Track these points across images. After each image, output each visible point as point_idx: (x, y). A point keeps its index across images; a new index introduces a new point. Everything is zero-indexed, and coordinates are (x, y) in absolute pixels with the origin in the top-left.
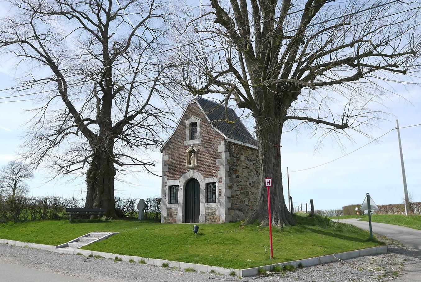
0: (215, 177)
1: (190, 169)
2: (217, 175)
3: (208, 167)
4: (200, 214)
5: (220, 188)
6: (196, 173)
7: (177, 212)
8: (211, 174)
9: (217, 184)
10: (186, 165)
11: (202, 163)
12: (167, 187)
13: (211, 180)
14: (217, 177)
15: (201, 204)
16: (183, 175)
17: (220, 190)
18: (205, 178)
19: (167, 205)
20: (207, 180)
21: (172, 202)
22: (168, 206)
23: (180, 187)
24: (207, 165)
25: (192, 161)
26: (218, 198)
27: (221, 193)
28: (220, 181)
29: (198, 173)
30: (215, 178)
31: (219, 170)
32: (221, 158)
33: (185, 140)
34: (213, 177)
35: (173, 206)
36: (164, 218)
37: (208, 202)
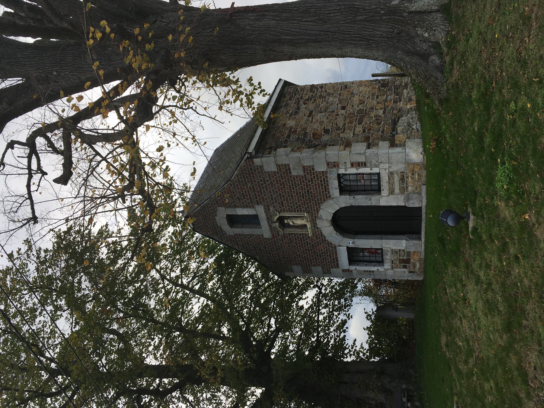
0: (327, 177)
1: (314, 226)
2: (323, 172)
3: (308, 191)
4: (403, 204)
5: (349, 165)
6: (321, 215)
8: (322, 185)
9: (342, 171)
10: (308, 234)
11: (302, 204)
12: (353, 268)
13: (334, 184)
14: (326, 172)
16: (327, 239)
17: (352, 165)
18: (330, 196)
19: (387, 269)
20: (335, 191)
21: (380, 259)
22: (387, 266)
23: (351, 245)
24: (305, 192)
25: (299, 222)
27: (359, 163)
28: (335, 166)
29: (321, 211)
30: (328, 175)
31: (313, 169)
32: (289, 165)
33: (262, 235)
34: (327, 181)
35: (388, 257)
36: (411, 274)
37: (378, 190)
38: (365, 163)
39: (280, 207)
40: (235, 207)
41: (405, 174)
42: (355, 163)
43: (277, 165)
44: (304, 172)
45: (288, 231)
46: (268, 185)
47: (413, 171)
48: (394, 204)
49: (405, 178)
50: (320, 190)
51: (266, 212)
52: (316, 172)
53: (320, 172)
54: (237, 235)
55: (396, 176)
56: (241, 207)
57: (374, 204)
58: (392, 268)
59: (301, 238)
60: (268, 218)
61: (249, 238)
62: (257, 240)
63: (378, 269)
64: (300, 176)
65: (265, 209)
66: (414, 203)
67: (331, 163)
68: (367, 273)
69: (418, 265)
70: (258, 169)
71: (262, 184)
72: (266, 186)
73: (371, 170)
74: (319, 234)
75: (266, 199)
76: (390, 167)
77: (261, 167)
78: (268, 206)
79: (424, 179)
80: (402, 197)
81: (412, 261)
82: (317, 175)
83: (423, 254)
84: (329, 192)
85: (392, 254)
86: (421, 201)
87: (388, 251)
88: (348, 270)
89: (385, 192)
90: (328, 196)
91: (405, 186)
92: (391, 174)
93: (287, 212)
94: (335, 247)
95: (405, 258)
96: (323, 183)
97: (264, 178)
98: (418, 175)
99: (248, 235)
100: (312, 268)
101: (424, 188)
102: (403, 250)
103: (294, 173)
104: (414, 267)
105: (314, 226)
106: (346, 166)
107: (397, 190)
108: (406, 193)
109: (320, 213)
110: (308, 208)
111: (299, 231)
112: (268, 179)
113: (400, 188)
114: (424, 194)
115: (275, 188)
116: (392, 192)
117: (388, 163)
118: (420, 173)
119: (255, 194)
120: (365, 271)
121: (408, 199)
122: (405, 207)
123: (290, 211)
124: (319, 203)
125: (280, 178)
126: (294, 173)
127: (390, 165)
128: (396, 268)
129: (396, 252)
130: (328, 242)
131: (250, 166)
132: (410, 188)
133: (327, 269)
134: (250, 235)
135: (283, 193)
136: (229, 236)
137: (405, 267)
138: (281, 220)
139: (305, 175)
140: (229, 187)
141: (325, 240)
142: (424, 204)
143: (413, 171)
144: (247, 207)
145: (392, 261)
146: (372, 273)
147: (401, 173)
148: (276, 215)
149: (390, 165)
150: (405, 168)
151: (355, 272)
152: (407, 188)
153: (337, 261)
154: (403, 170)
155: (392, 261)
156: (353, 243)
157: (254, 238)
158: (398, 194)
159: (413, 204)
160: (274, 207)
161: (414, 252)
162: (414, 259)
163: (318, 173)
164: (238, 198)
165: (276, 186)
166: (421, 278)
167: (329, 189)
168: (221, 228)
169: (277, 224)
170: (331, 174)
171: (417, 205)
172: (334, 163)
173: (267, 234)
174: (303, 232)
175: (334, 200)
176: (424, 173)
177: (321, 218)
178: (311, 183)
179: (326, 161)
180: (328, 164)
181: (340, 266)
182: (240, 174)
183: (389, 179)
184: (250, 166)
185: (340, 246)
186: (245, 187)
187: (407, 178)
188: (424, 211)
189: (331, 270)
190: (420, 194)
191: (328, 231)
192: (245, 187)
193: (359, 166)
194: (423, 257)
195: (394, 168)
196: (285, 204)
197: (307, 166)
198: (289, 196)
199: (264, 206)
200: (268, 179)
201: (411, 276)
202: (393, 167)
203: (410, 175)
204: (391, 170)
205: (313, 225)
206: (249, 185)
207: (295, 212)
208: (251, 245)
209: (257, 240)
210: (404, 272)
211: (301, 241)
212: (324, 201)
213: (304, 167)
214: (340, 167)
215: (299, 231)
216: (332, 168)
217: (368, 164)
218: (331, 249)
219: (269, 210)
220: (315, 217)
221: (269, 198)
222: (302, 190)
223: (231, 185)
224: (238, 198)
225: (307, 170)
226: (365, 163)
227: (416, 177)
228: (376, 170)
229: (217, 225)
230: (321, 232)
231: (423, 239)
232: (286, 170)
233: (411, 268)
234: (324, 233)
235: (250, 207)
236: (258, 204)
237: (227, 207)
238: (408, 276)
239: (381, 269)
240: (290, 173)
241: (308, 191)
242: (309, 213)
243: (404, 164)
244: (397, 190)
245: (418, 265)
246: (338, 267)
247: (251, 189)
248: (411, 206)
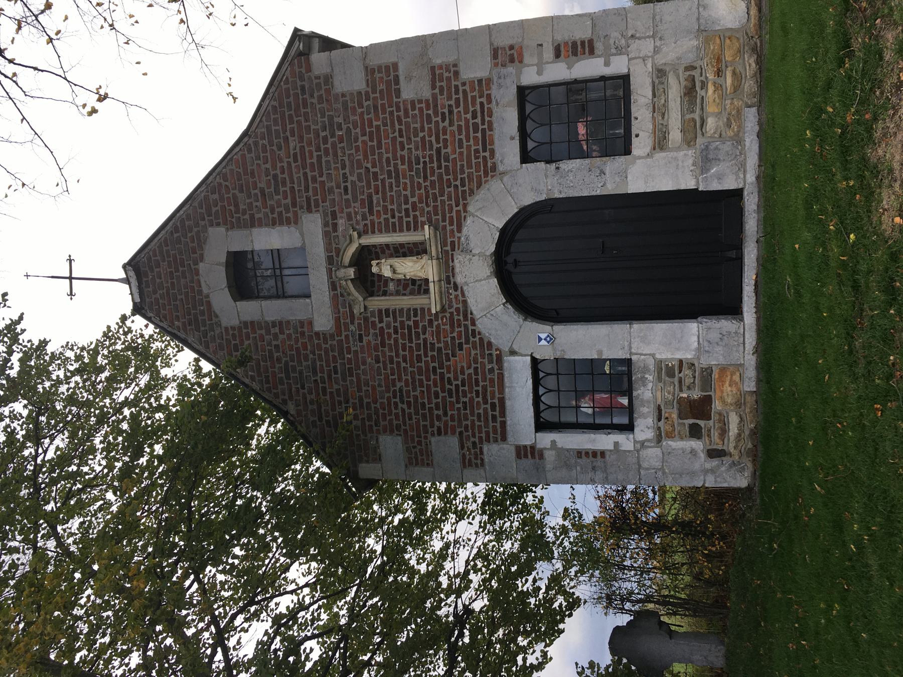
0: (489, 97)
2: (480, 81)
3: (438, 151)
5: (549, 54)
7: (681, 361)
8: (475, 126)
9: (530, 77)
10: (429, 309)
11: (421, 202)
12: (545, 439)
13: (507, 120)
14: (489, 81)
15: (637, 184)
17: (558, 55)
18: (494, 168)
19: (642, 443)
20: (508, 151)
21: (625, 421)
22: (644, 429)
23: (544, 352)
24: (431, 156)
25: (409, 267)
26: (601, 61)
27: (574, 44)
28: (512, 60)
29: (469, 220)
30: (495, 92)
31: (456, 74)
32: (395, 66)
33: (310, 323)
35: (647, 392)
36: (715, 462)
37: (622, 146)
38: (591, 42)
39: (364, 218)
40: (253, 223)
41: (696, 73)
42: (566, 44)
44: (433, 87)
45: (378, 303)
47: (719, 60)
48: (666, 184)
49: (698, 85)
50: (469, 147)
51: (326, 234)
52: (464, 84)
53: (472, 82)
54: (245, 323)
55: (672, 80)
56: (267, 225)
57: (611, 188)
58: (659, 439)
59: (409, 328)
60: (330, 260)
61: (276, 336)
62: (297, 341)
63: (616, 444)
64: (420, 102)
65: (326, 224)
66: (721, 179)
67: (504, 49)
68: (584, 461)
72: (334, 146)
73: (607, 64)
75: (331, 191)
76: (657, 50)
77: (328, 79)
78: (334, 216)
79: (749, 85)
80: (688, 157)
81: (717, 406)
82: (465, 91)
83: (751, 372)
84: (492, 152)
85: (660, 379)
86: (743, 166)
87: (646, 369)
88: (533, 447)
89: (641, 145)
90: (490, 170)
91: (696, 116)
92: (660, 73)
93: (380, 231)
95: (696, 394)
96: (478, 120)
97: (331, 118)
99: (274, 324)
100: (433, 440)
101: (751, 118)
102: (692, 365)
103: (408, 92)
104: (724, 432)
106: (540, 55)
107: (675, 135)
108: (700, 140)
109: (465, 230)
110: (436, 214)
112: (341, 120)
113: (683, 122)
114: (751, 144)
116: (660, 143)
117: (653, 36)
118: (739, 69)
119: (305, 174)
120: (579, 453)
121: (705, 161)
123: (387, 231)
124: (464, 192)
125: (372, 115)
126: (408, 92)
127: (658, 43)
128: (670, 436)
129: (670, 373)
130: (481, 339)
131: (302, 78)
132: (711, 122)
133: (474, 443)
134: (281, 323)
135: (374, 166)
136: (226, 329)
137: (695, 432)
138: (364, 258)
139: (434, 97)
140: (243, 156)
141: (473, 331)
142: (751, 177)
143: (719, 60)
144: (281, 224)
146: (599, 462)
149: (658, 43)
151: (550, 456)
153: (503, 413)
154: (690, 58)
157: (289, 337)
158: (678, 149)
159: (720, 177)
160: (349, 217)
161: (723, 369)
162: (724, 396)
163: (467, 88)
164: (262, 191)
165: (359, 143)
166: (741, 481)
167: (492, 143)
168: (209, 304)
169: (351, 272)
170: (500, 86)
171: (730, 184)
172: (511, 47)
173: (323, 322)
174: (417, 301)
175: (505, 179)
176: (750, 64)
179: (491, 44)
180: (495, 53)
181: (510, 438)
182: (274, 107)
183: (654, 95)
184: (302, 78)
185: (513, 353)
186: (282, 153)
187: (704, 85)
188: (751, 203)
190: (738, 140)
192: (282, 153)
193: (575, 54)
194: (750, 385)
196: (378, 203)
197: (440, 67)
198: (390, 177)
199: (325, 215)
200: (341, 120)
201: (712, 471)
202: (665, 49)
203: (711, 76)
204: (660, 60)
205: (444, 277)
206: (292, 145)
207: (401, 230)
208: (279, 360)
209: (297, 341)
210: (693, 452)
211: (411, 341)
213: (433, 69)
214: (527, 59)
216: (504, 65)
217: (599, 46)
219: (335, 226)
220: (453, 243)
221: (338, 187)
222: (424, 149)
223: (250, 151)
224: (262, 191)
225: (441, 75)
226: (591, 42)
228: (618, 66)
229: (200, 292)
230: (465, 302)
232: (388, 83)
233: (715, 435)
234: (471, 302)
235: (288, 222)
236: (309, 210)
237: (232, 227)
238: (706, 472)
239: (625, 441)
240: (398, 92)
241: (438, 151)
242: (436, 229)
243: (697, 37)
244: (675, 135)
246: (504, 438)
247: (296, 161)
248: (715, 186)
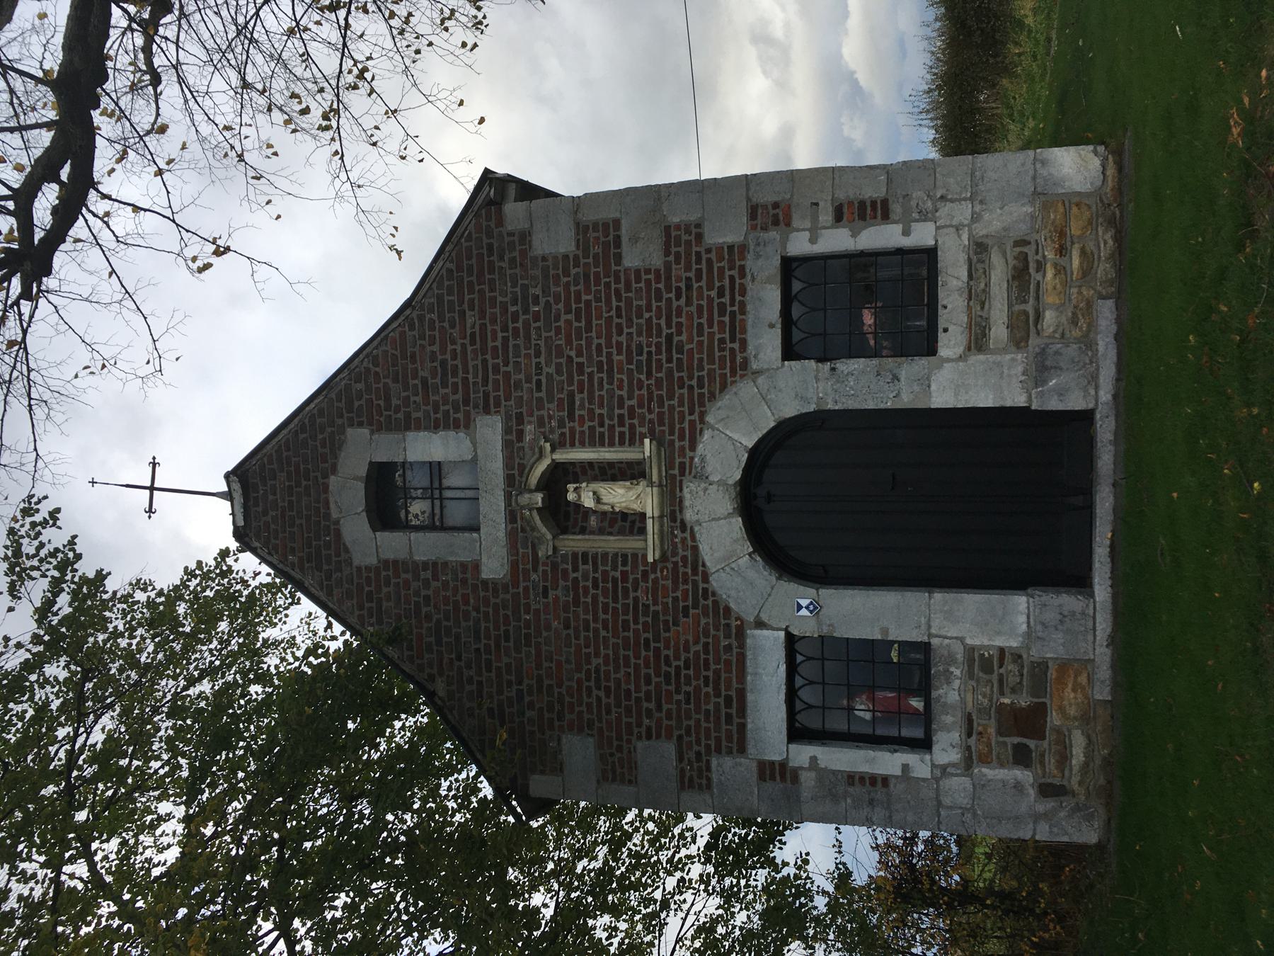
1: (674, 519)
2: (731, 248)
3: (669, 338)
4: (1019, 400)
5: (826, 217)
6: (703, 460)
7: (1002, 651)
8: (722, 307)
9: (800, 245)
10: (645, 556)
11: (641, 406)
12: (802, 754)
13: (766, 301)
14: (743, 248)
15: (943, 396)
16: (715, 582)
17: (839, 217)
18: (745, 364)
19: (944, 768)
20: (766, 344)
21: (918, 733)
22: (947, 749)
24: (658, 345)
25: (618, 496)
26: (898, 228)
27: (862, 204)
28: (776, 223)
29: (707, 435)
30: (749, 263)
31: (699, 237)
32: (617, 223)
33: (477, 566)
34: (743, 292)
35: (952, 693)
36: (1050, 804)
38: (885, 202)
39: (561, 424)
40: (409, 425)
41: (1030, 250)
42: (851, 203)
43: (577, 224)
44: (667, 253)
45: (574, 543)
46: (537, 317)
47: (1062, 234)
48: (985, 399)
49: (1032, 266)
50: (711, 335)
51: (507, 445)
52: (708, 251)
53: (720, 249)
54: (386, 562)
55: (996, 259)
56: (427, 428)
57: (907, 399)
58: (968, 763)
59: (615, 580)
60: (510, 480)
61: (426, 583)
62: (456, 590)
63: (905, 767)
64: (648, 271)
65: (507, 431)
66: (1063, 394)
67: (765, 207)
68: (856, 790)
69: (1078, 744)
70: (512, 246)
71: (515, 318)
72: (527, 325)
73: (906, 233)
74: (684, 558)
75: (518, 385)
76: (976, 218)
77: (525, 236)
78: (520, 419)
79: (1104, 269)
80: (1016, 364)
81: (1054, 719)
82: (709, 261)
83: (1104, 672)
84: (744, 344)
85: (971, 675)
86: (1094, 379)
87: (951, 660)
88: (783, 765)
89: (951, 343)
90: (740, 367)
91: (1029, 308)
92: (980, 249)
93: (583, 444)
94: (741, 634)
95: (1024, 701)
96: (726, 299)
97: (525, 288)
98: (1083, 252)
99: (425, 565)
100: (640, 745)
101: (1106, 313)
102: (1017, 657)
103: (632, 259)
104: (1064, 759)
105: (674, 519)
106: (815, 219)
107: (999, 332)
108: (1034, 341)
109: (700, 448)
110: (661, 423)
111: (613, 543)
112: (538, 291)
113: (1010, 316)
114: (1106, 346)
115: (558, 330)
116: (978, 341)
117: (971, 199)
118: (1091, 246)
119: (485, 361)
120: (851, 778)
121: (1040, 370)
122: (1026, 410)
123: (592, 444)
124: (701, 396)
125: (581, 287)
126: (632, 259)
127: (978, 208)
128: (985, 760)
129: (986, 665)
130: (716, 603)
131: (489, 234)
132: (1049, 316)
133: (698, 754)
134: (435, 564)
135: (579, 354)
136: (359, 569)
137: (1022, 757)
138: (559, 477)
139: (668, 266)
140: (403, 334)
141: (705, 590)
142: (1105, 395)
143: (1062, 234)
144: (447, 427)
145: (970, 721)
146: (879, 793)
147: (1017, 243)
148: (541, 456)
149: (978, 208)
150: (1033, 217)
151: (808, 779)
152: (1038, 317)
153: (742, 711)
154: (1022, 229)
155: (970, 721)
156: (815, 608)
157: (445, 585)
158: (1004, 351)
159: (1061, 393)
160: (541, 423)
161: (1064, 666)
162: (1065, 706)
163: (713, 256)
164: (424, 382)
165: (562, 323)
166: (1089, 835)
167: (744, 331)
168: (338, 534)
169: (539, 498)
170: (758, 256)
171: (1076, 402)
172: (776, 205)
173: (494, 566)
174: (629, 544)
175: (760, 380)
176: (1105, 241)
177: (702, 477)
178: (683, 301)
179: (749, 199)
180: (753, 212)
181: (751, 750)
182: (450, 271)
183: (970, 276)
184: (489, 234)
185: (760, 624)
186: (456, 333)
187: (1040, 267)
188: (1105, 430)
189: (714, 763)
190: (1088, 343)
191: (720, 535)
192: (456, 333)
193: (862, 217)
194: (1102, 693)
195: (995, 221)
196: (582, 406)
197: (678, 227)
198: (600, 370)
199: (508, 418)
200: (538, 291)
201: (1045, 816)
202: (986, 216)
203: (1050, 255)
204: (980, 230)
205: (667, 510)
206: (469, 321)
207: (612, 444)
208: (428, 617)
209: (456, 590)
210: (1018, 786)
211: (615, 600)
212: (723, 387)
213: (667, 228)
214: (796, 223)
215: (613, 543)
216: (764, 229)
217: (896, 209)
218: (724, 643)
219: (520, 434)
220: (682, 466)
221: (528, 381)
222: (649, 335)
223: (412, 327)
224: (424, 382)
225: (678, 238)
226: (885, 202)
227: (1076, 262)
228: (923, 235)
229: (327, 516)
230: (695, 549)
231: (1102, 590)
232: (606, 246)
233: (1051, 762)
234: (704, 548)
235: (457, 426)
236: (487, 411)
237: (379, 430)
238: (1037, 818)
239: (919, 765)
240: (619, 258)
241: (669, 338)
242: (660, 444)
243: (1032, 203)
244: (999, 332)
245: (1078, 744)
246: (742, 750)
247: (473, 342)
248: (1054, 404)
